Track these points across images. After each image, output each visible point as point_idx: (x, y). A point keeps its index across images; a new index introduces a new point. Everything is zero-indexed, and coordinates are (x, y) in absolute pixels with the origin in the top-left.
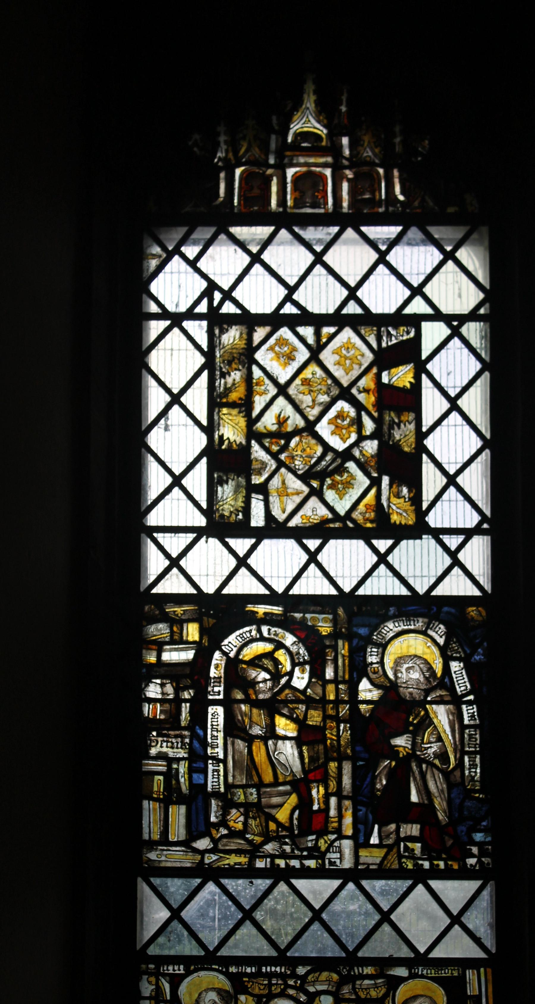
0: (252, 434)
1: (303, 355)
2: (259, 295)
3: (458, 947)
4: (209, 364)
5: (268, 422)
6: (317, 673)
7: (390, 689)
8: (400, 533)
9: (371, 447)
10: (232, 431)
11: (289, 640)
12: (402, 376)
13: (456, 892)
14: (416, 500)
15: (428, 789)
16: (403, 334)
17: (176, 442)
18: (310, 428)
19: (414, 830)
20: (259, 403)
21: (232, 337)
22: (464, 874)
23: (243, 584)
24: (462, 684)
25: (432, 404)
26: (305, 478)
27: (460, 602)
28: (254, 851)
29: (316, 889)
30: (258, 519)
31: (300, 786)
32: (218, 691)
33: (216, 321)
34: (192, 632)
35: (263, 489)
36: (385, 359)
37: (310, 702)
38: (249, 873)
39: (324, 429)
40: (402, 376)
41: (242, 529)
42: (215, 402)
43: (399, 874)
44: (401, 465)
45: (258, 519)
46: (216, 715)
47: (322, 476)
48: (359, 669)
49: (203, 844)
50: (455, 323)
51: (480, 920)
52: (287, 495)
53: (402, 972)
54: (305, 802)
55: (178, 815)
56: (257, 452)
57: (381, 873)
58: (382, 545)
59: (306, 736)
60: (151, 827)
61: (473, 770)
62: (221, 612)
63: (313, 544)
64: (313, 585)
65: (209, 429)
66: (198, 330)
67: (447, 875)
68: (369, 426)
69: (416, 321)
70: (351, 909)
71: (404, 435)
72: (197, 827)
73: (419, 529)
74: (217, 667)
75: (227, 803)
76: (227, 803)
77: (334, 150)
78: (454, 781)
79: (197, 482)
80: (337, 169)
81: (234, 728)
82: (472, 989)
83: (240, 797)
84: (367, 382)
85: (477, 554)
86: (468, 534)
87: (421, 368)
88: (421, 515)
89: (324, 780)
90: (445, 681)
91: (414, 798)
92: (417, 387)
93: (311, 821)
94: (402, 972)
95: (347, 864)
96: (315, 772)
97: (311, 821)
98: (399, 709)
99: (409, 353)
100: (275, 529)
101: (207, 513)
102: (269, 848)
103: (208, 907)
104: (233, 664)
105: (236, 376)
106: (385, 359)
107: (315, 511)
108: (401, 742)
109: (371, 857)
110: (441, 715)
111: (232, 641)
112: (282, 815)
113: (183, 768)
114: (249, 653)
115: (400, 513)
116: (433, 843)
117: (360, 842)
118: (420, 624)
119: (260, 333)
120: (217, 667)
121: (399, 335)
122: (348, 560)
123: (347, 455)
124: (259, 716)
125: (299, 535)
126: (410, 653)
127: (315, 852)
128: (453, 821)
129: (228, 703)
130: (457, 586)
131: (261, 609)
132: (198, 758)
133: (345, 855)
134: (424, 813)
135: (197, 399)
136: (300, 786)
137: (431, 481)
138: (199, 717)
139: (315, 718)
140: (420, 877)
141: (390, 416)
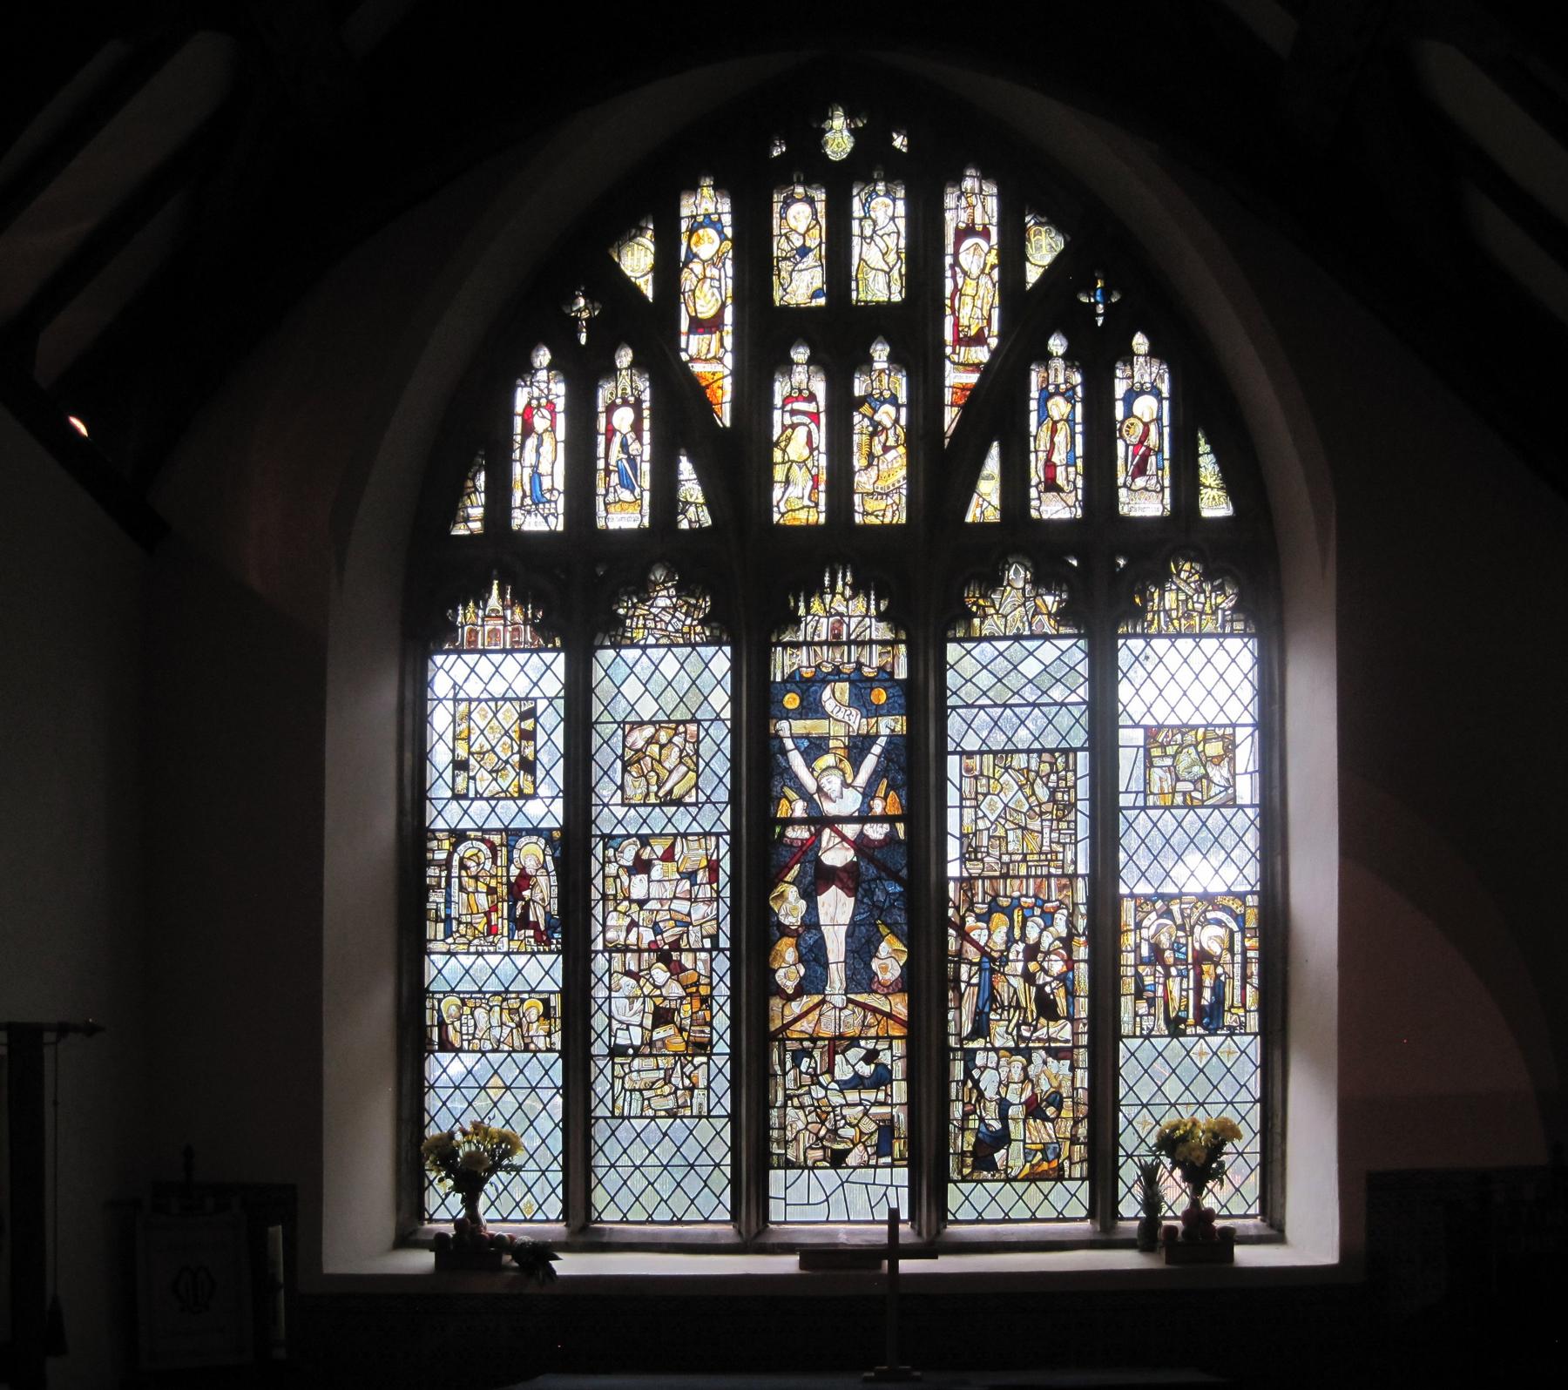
0: (470, 753)
1: (491, 715)
2: (473, 688)
3: (548, 985)
4: (454, 721)
5: (475, 748)
6: (494, 862)
7: (523, 869)
8: (527, 797)
9: (516, 758)
10: (462, 752)
11: (483, 847)
12: (528, 725)
13: (547, 960)
14: (534, 782)
15: (537, 914)
16: (529, 705)
17: (441, 756)
18: (493, 749)
19: (531, 933)
20: (473, 738)
21: (463, 707)
22: (551, 952)
23: (466, 824)
24: (551, 867)
25: (541, 737)
26: (490, 772)
27: (551, 830)
28: (469, 943)
29: (494, 960)
30: (472, 794)
31: (487, 914)
32: (455, 872)
33: (456, 700)
34: (446, 845)
35: (474, 778)
36: (523, 716)
37: (492, 876)
38: (468, 953)
39: (498, 749)
40: (528, 725)
41: (465, 797)
42: (455, 739)
43: (526, 953)
44: (528, 766)
45: (472, 794)
46: (455, 881)
47: (497, 771)
48: (510, 860)
49: (450, 940)
50: (551, 700)
51: (558, 973)
52: (484, 782)
53: (525, 996)
54: (489, 922)
55: (441, 926)
56: (472, 761)
57: (518, 953)
58: (520, 803)
59: (491, 891)
60: (430, 934)
61: (554, 907)
62: (458, 836)
63: (493, 803)
64: (494, 823)
65: (453, 751)
66: (450, 704)
67: (545, 952)
68: (516, 748)
69: (535, 700)
70: (507, 968)
71: (529, 753)
72: (448, 933)
73: (534, 796)
74: (456, 862)
75: (460, 923)
76: (460, 923)
77: (504, 617)
78: (548, 914)
79: (448, 775)
80: (505, 626)
81: (462, 888)
82: (552, 1004)
83: (464, 919)
84: (515, 727)
85: (558, 807)
86: (554, 798)
87: (537, 720)
88: (536, 788)
89: (496, 911)
90: (544, 866)
91: (532, 918)
92: (535, 729)
93: (492, 930)
94: (525, 996)
95: (505, 949)
96: (494, 908)
97: (492, 930)
98: (525, 879)
99: (531, 714)
100: (479, 796)
101: (453, 789)
102: (476, 942)
103: (453, 969)
104: (462, 859)
105: (464, 726)
106: (523, 716)
107: (494, 788)
108: (526, 893)
109: (514, 945)
110: (542, 880)
111: (461, 848)
112: (480, 927)
113: (442, 907)
114: (467, 855)
115: (528, 790)
116: (538, 942)
117: (511, 939)
118: (534, 839)
119: (474, 704)
120: (456, 862)
121: (528, 706)
122: (507, 809)
123: (507, 762)
124: (472, 882)
125: (487, 799)
126: (531, 854)
127: (492, 944)
128: (547, 929)
129: (460, 877)
130: (549, 823)
131: (472, 834)
132: (448, 903)
133: (504, 945)
134: (535, 926)
135: (449, 737)
136: (487, 914)
137: (540, 773)
138: (449, 884)
139: (493, 883)
140: (533, 954)
141: (524, 743)
